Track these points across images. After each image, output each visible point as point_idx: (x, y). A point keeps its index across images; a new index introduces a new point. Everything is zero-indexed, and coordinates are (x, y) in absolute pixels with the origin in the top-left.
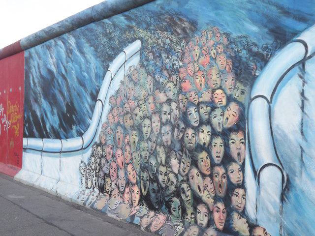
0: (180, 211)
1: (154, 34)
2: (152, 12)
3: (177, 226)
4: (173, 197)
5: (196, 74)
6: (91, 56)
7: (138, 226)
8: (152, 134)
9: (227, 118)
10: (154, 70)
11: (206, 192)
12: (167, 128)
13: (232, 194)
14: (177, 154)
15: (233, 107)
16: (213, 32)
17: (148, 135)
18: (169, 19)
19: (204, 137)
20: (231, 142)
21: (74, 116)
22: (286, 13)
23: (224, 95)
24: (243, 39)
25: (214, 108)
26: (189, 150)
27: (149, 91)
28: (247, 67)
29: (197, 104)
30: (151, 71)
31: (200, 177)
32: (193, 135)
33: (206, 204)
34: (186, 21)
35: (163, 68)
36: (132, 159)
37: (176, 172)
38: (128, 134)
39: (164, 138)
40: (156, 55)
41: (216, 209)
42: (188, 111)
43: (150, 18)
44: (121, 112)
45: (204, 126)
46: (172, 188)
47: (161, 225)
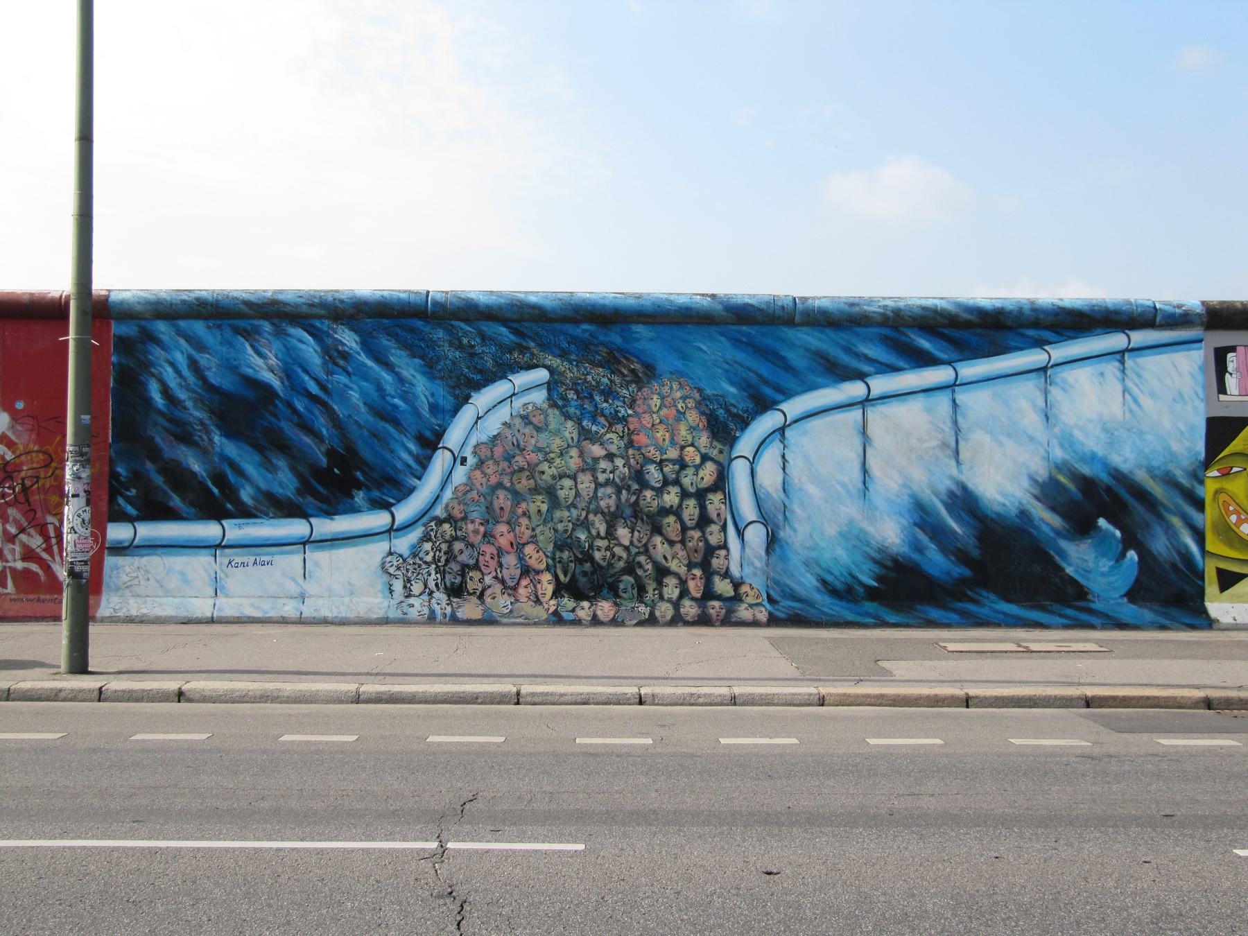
0: (635, 592)
1: (577, 366)
2: (571, 336)
5: (656, 427)
9: (703, 478)
11: (676, 561)
12: (609, 490)
13: (712, 557)
14: (628, 522)
16: (680, 384)
18: (606, 353)
19: (671, 497)
20: (707, 502)
21: (358, 474)
22: (766, 382)
23: (697, 453)
25: (683, 466)
27: (570, 441)
28: (726, 427)
31: (666, 545)
33: (676, 575)
37: (627, 543)
38: (525, 500)
39: (602, 504)
41: (692, 576)
43: (569, 343)
46: (621, 564)
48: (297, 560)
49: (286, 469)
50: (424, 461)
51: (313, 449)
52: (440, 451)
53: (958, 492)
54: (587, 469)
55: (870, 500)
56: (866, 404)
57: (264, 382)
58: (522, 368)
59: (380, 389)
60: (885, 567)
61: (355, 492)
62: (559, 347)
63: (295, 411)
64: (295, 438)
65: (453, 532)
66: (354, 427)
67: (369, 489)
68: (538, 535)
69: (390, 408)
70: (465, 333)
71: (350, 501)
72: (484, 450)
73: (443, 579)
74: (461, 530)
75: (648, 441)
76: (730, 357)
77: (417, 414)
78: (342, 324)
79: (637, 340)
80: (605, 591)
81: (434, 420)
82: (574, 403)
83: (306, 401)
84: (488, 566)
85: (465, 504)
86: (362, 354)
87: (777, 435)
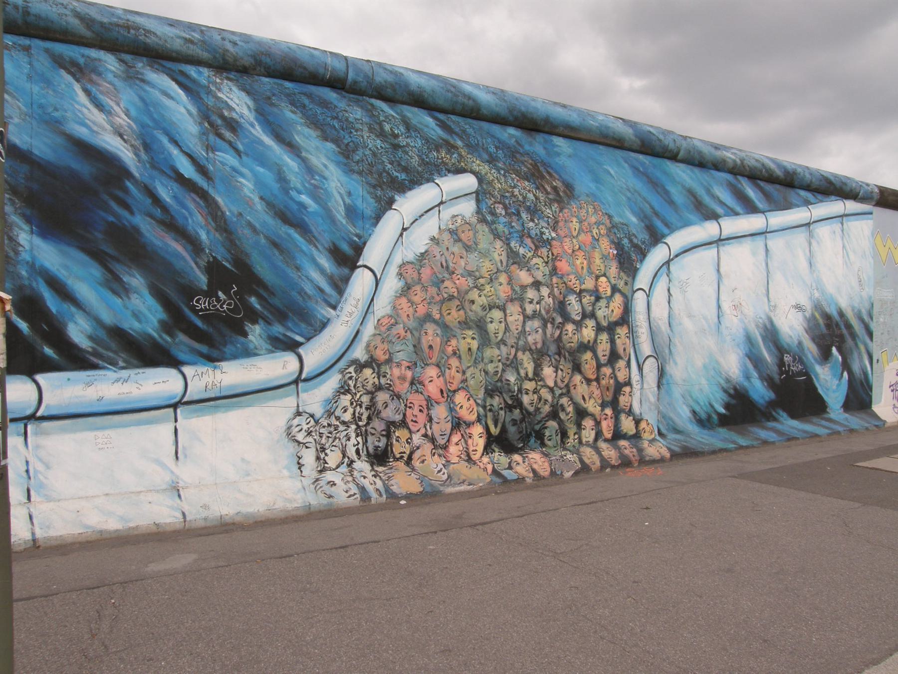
1: (504, 176)
2: (499, 141)
3: (566, 456)
4: (547, 421)
6: (324, 161)
7: (521, 480)
8: (508, 334)
9: (613, 311)
10: (507, 232)
11: (592, 401)
12: (536, 323)
13: (620, 394)
14: (553, 360)
15: (618, 299)
16: (594, 208)
17: (500, 336)
18: (531, 164)
20: (616, 337)
21: (253, 300)
22: (656, 214)
23: (608, 284)
24: (624, 226)
25: (598, 298)
26: (568, 352)
27: (499, 264)
28: (629, 257)
29: (578, 291)
30: (501, 234)
31: (585, 386)
32: (574, 331)
33: (592, 415)
34: (558, 180)
35: (524, 234)
36: (465, 381)
37: (551, 383)
38: (455, 336)
39: (530, 339)
40: (509, 211)
41: (605, 416)
42: (566, 299)
43: (496, 147)
45: (588, 319)
46: (547, 409)
47: (546, 464)
48: (165, 431)
49: (145, 292)
50: (340, 283)
51: (185, 261)
52: (359, 271)
53: (769, 326)
54: (515, 299)
55: (722, 333)
56: (720, 243)
57: (108, 152)
58: (449, 171)
59: (282, 178)
60: (730, 395)
61: (249, 327)
62: (486, 150)
63: (156, 200)
64: (158, 243)
65: (376, 380)
66: (247, 232)
67: (268, 322)
69: (295, 207)
70: (386, 117)
71: (242, 339)
72: (410, 271)
73: (365, 442)
74: (385, 376)
75: (569, 268)
76: (632, 185)
77: (333, 220)
78: (228, 79)
79: (558, 154)
80: (533, 440)
81: (351, 229)
82: (502, 220)
83: (175, 186)
84: (416, 422)
85: (390, 342)
86: (258, 127)
87: (665, 268)
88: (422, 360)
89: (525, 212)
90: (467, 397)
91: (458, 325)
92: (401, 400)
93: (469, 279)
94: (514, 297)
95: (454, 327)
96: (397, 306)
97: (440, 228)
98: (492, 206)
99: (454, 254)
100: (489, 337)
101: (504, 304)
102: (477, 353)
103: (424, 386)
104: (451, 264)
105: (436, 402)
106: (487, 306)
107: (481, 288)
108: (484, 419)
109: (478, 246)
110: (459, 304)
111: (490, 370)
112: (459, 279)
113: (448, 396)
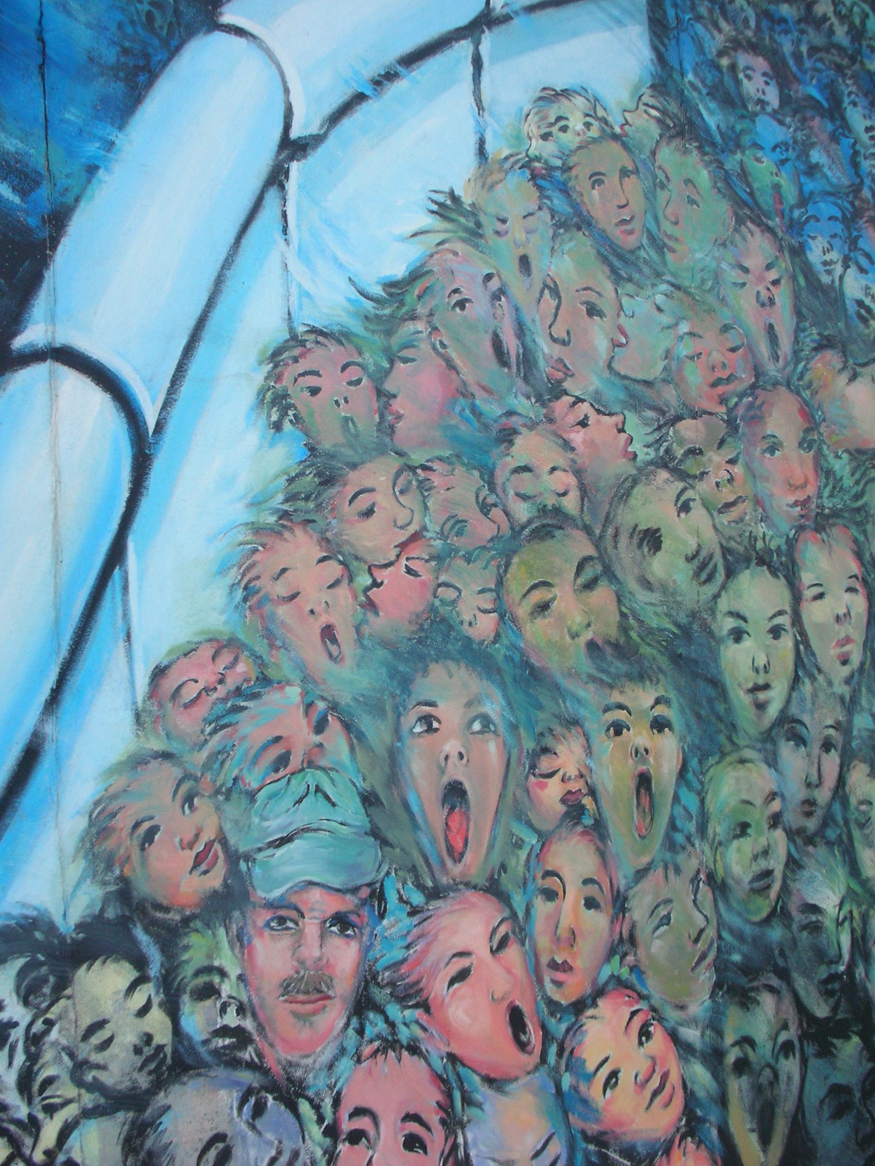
8: (807, 687)
10: (790, 194)
17: (776, 699)
27: (764, 349)
30: (766, 200)
38: (574, 723)
44: (472, 514)
54: (836, 514)
68: (642, 935)
74: (208, 992)
88: (413, 869)
89: (862, 101)
90: (637, 1022)
91: (586, 665)
92: (304, 1107)
93: (632, 420)
94: (828, 503)
95: (572, 674)
96: (266, 585)
97: (481, 151)
98: (725, 62)
99: (555, 292)
100: (729, 710)
101: (791, 543)
102: (676, 799)
103: (425, 1006)
104: (544, 347)
105: (489, 1081)
106: (718, 558)
107: (691, 466)
108: (713, 1117)
109: (669, 257)
110: (591, 551)
111: (737, 870)
112: (583, 423)
113: (547, 1037)
